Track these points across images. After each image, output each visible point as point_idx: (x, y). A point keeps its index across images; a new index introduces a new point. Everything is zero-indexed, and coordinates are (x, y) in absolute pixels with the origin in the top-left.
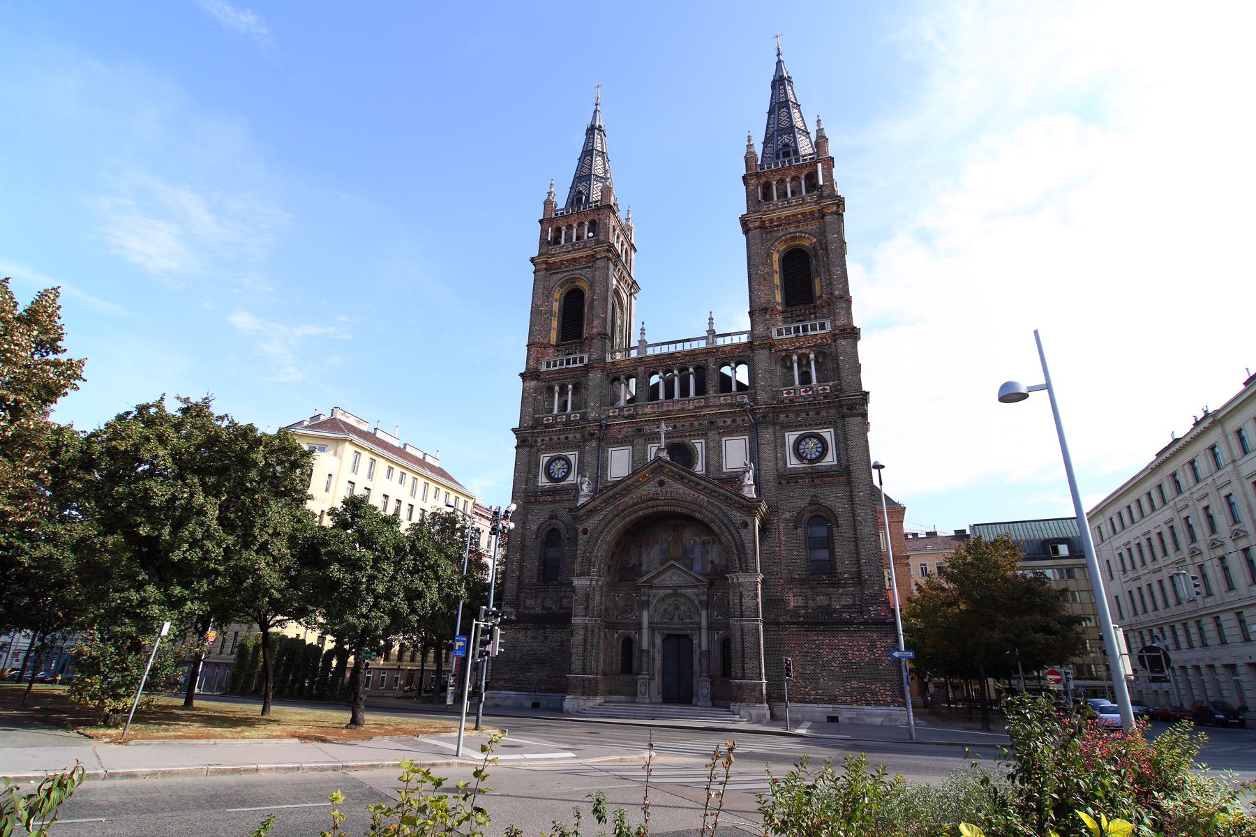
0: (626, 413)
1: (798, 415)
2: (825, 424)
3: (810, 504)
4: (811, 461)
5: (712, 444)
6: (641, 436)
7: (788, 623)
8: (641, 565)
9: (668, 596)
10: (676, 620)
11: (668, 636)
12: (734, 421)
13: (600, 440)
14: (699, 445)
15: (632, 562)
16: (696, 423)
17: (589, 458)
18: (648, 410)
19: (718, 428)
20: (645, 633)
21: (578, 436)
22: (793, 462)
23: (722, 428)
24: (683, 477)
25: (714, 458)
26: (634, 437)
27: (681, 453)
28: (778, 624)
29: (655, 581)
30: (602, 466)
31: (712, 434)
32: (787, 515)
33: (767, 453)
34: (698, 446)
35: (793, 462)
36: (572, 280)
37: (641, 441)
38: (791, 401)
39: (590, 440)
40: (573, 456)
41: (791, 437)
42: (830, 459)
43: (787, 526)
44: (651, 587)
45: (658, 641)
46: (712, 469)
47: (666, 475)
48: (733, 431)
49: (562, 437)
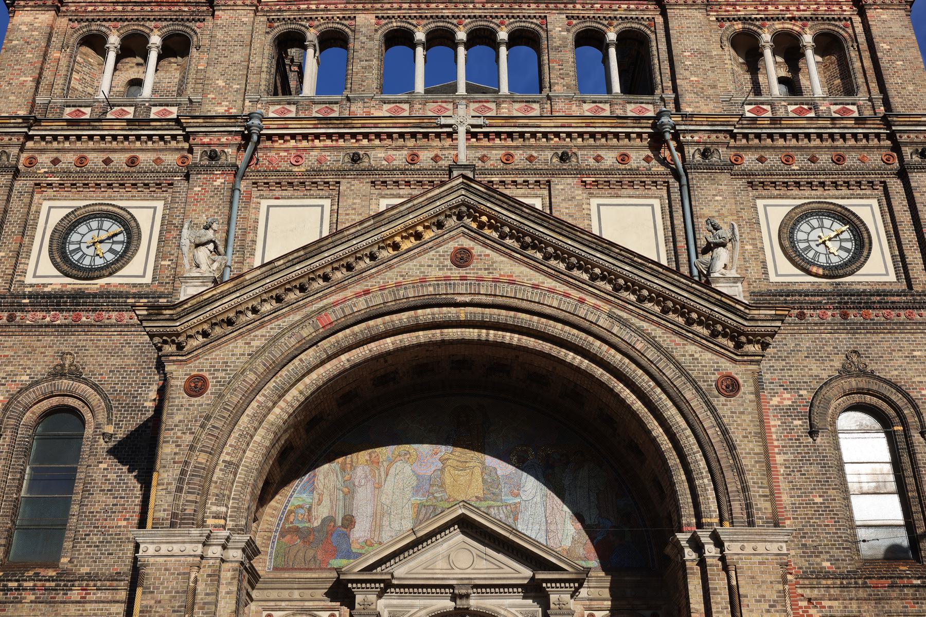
1: (788, 160)
2: (859, 183)
3: (845, 372)
4: (832, 272)
13: (237, 173)
29: (402, 570)
32: (787, 399)
39: (208, 169)
42: (878, 269)
43: (787, 428)
49: (120, 159)
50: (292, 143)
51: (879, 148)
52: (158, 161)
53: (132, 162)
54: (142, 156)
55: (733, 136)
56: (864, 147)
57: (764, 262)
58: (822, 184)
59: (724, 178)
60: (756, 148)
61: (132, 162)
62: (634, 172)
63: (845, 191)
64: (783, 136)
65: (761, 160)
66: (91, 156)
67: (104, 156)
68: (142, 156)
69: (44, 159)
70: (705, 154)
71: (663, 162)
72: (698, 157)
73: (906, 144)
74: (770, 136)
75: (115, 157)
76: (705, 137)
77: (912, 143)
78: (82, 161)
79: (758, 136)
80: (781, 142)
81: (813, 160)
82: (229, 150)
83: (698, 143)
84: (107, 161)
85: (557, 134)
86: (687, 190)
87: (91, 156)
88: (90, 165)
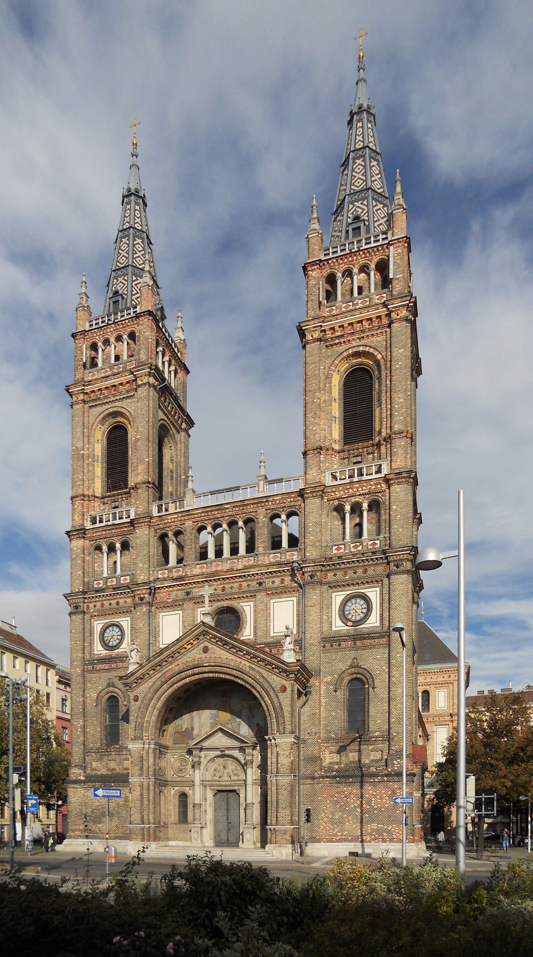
0: (175, 575)
1: (345, 574)
4: (356, 623)
5: (261, 607)
6: (191, 599)
7: (323, 777)
8: (192, 729)
9: (217, 757)
10: (226, 778)
11: (219, 791)
12: (282, 581)
13: (150, 605)
14: (247, 608)
15: (185, 726)
16: (244, 584)
17: (142, 625)
18: (197, 570)
19: (266, 590)
20: (198, 788)
21: (129, 600)
22: (338, 625)
23: (270, 589)
24: (227, 643)
25: (261, 625)
26: (184, 600)
27: (228, 619)
28: (313, 778)
30: (153, 632)
31: (261, 596)
33: (313, 615)
34: (247, 609)
35: (338, 625)
36: (115, 414)
37: (189, 605)
38: (340, 557)
39: (140, 605)
40: (125, 622)
41: (338, 597)
44: (201, 749)
45: (210, 794)
46: (259, 633)
47: (209, 641)
48: (280, 592)
49: (114, 602)
50: (167, 589)
51: (382, 563)
52: (125, 602)
53: (118, 603)
54: (120, 601)
55: (323, 566)
56: (376, 564)
57: (331, 622)
58: (358, 584)
59: (318, 587)
60: (333, 570)
61: (118, 603)
62: (286, 587)
63: (367, 585)
64: (343, 563)
65: (335, 575)
66: (105, 602)
67: (109, 602)
68: (120, 601)
69: (91, 605)
70: (312, 577)
71: (296, 582)
72: (309, 578)
73: (392, 561)
74: (338, 564)
75: (112, 602)
76: (312, 569)
77: (394, 561)
78: (103, 605)
79: (333, 564)
80: (343, 566)
81: (355, 573)
82: (146, 596)
83: (309, 572)
84: (110, 604)
85: (257, 574)
86: (304, 593)
87: (105, 602)
88: (105, 606)
